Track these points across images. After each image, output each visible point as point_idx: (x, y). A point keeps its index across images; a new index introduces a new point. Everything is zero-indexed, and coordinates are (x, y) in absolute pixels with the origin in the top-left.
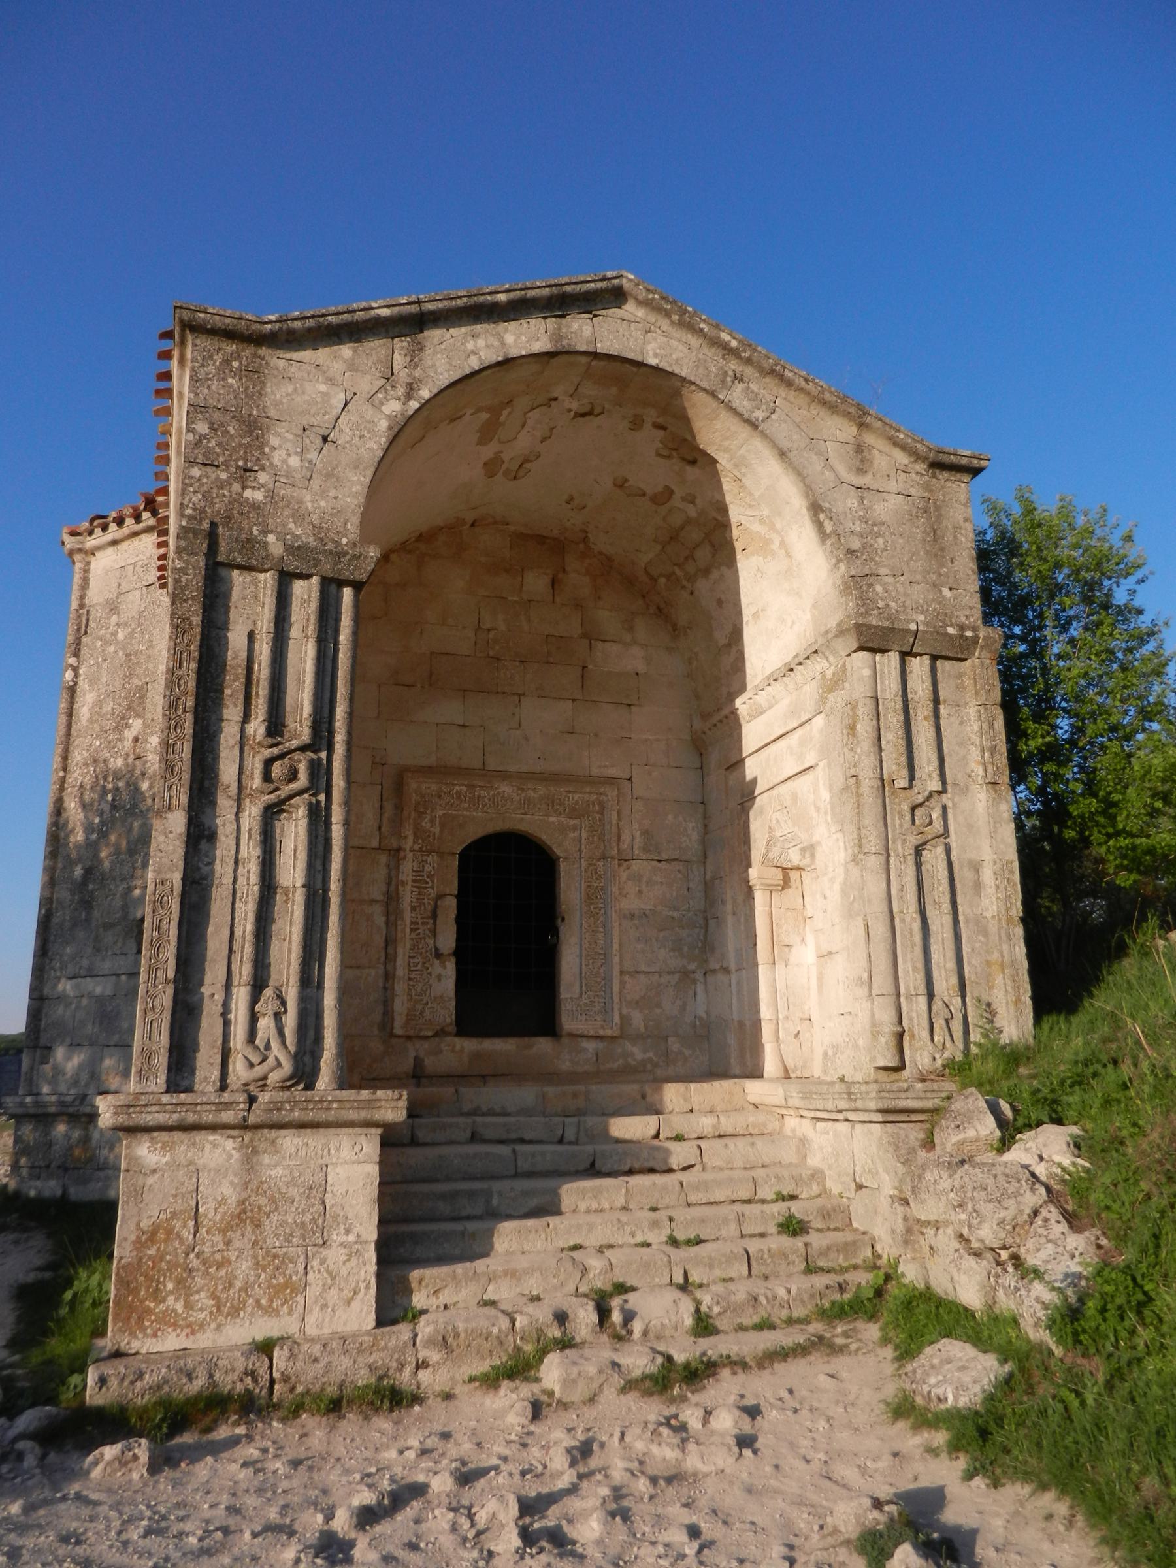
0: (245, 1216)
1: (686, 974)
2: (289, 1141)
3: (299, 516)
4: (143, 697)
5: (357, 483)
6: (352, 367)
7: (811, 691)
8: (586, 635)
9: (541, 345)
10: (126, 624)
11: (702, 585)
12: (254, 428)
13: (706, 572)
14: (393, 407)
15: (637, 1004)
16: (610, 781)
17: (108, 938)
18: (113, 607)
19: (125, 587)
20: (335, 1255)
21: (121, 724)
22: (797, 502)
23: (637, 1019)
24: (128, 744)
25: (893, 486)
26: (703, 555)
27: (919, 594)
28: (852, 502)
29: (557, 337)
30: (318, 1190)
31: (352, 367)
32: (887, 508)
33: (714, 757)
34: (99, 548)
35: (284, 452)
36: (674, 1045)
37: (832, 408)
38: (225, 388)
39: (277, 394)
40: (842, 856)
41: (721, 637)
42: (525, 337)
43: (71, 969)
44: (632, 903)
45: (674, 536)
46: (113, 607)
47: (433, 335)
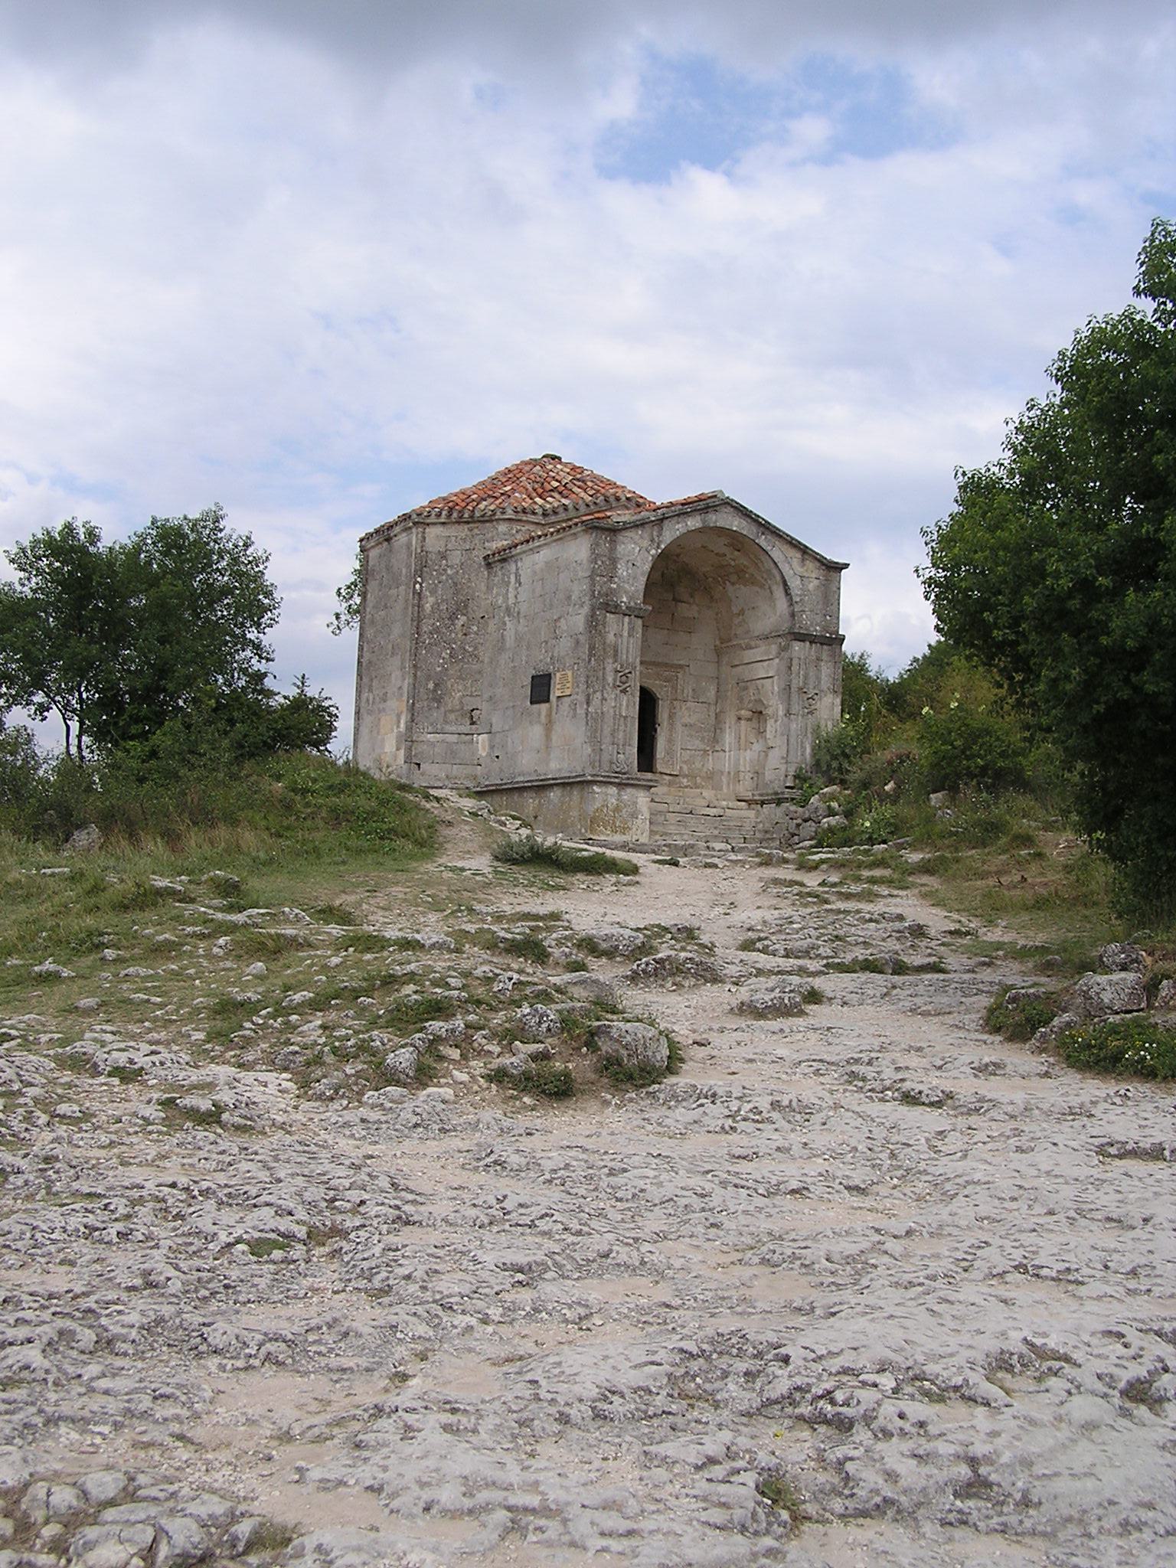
0: (617, 809)
1: (705, 751)
2: (629, 790)
3: (626, 592)
4: (466, 606)
5: (643, 580)
6: (641, 537)
7: (774, 648)
8: (674, 599)
9: (699, 525)
10: (452, 567)
11: (730, 588)
12: (614, 561)
13: (733, 584)
14: (653, 552)
15: (685, 762)
16: (681, 667)
17: (452, 717)
18: (443, 556)
19: (450, 546)
20: (639, 821)
21: (453, 617)
22: (778, 578)
23: (685, 767)
24: (459, 626)
25: (814, 575)
26: (734, 578)
27: (818, 619)
28: (798, 582)
29: (704, 521)
30: (636, 803)
31: (641, 537)
32: (812, 585)
33: (725, 660)
34: (434, 524)
35: (622, 570)
36: (699, 780)
37: (795, 546)
38: (604, 547)
39: (620, 548)
40: (781, 713)
41: (735, 610)
42: (694, 523)
43: (430, 729)
44: (686, 720)
45: (722, 567)
46: (443, 556)
47: (666, 522)
